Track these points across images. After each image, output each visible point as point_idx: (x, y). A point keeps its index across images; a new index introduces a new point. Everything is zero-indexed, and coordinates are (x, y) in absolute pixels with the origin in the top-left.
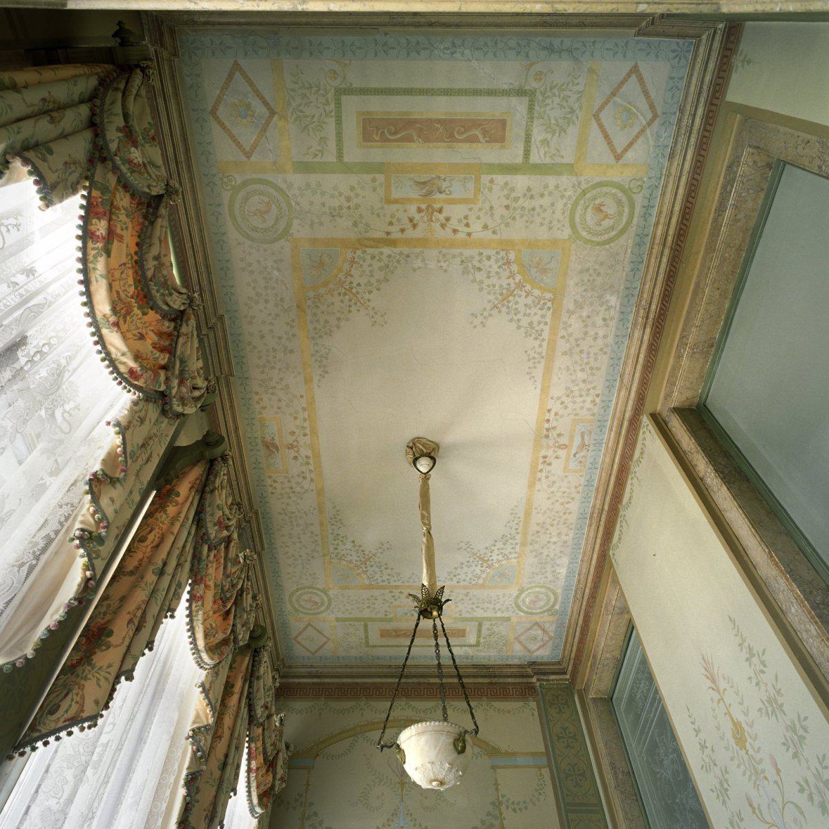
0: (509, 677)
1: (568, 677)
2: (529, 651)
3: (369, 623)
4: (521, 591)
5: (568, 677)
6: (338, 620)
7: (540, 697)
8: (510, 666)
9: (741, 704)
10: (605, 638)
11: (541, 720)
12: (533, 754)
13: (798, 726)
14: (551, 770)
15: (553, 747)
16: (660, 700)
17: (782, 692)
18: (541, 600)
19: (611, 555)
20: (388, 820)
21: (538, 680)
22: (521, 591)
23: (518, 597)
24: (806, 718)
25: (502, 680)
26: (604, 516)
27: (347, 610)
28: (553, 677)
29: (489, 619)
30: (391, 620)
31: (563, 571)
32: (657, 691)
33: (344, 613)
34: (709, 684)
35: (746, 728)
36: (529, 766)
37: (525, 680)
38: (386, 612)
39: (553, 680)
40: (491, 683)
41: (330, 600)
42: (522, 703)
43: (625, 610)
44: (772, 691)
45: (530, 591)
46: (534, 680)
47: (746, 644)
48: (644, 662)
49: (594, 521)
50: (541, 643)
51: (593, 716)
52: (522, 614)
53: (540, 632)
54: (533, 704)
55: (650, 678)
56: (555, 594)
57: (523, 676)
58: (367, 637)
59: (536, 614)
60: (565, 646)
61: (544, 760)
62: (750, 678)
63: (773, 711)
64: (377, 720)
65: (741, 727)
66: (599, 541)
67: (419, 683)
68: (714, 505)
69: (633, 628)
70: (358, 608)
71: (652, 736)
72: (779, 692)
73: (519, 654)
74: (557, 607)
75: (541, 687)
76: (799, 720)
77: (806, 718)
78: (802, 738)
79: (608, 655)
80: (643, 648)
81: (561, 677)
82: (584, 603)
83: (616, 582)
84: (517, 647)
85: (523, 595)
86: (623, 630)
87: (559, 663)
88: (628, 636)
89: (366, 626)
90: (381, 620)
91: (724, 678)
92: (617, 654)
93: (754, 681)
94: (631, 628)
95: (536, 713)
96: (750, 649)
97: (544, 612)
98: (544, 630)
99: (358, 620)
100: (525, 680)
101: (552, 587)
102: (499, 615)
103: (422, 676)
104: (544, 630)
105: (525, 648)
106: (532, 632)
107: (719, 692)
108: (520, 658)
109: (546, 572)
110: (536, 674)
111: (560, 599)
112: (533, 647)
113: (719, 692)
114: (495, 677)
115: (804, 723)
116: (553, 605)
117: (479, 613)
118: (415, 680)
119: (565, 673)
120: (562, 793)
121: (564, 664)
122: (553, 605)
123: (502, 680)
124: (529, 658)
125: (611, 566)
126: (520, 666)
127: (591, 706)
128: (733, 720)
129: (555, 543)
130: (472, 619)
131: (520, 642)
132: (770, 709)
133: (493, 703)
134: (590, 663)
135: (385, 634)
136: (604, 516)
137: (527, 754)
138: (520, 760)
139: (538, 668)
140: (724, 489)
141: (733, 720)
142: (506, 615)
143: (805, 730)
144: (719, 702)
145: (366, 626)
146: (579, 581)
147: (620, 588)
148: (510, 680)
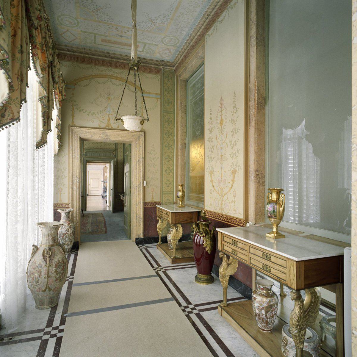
0: (152, 64)
1: (174, 68)
2: (162, 57)
3: (96, 35)
4: (165, 37)
5: (174, 68)
6: (82, 31)
7: (162, 74)
8: (153, 60)
9: (226, 116)
10: (192, 63)
11: (161, 82)
12: (156, 94)
13: (237, 130)
14: (161, 100)
15: (163, 93)
16: (204, 92)
17: (237, 120)
18: (172, 41)
19: (206, 38)
20: (104, 109)
21: (163, 68)
22: (165, 37)
23: (164, 38)
24: (239, 130)
25: (149, 65)
26: (209, 19)
27: (86, 28)
28: (168, 67)
29: (149, 44)
30: (106, 36)
31: (184, 33)
32: (203, 89)
33: (85, 29)
34: (220, 105)
35: (224, 122)
36: (154, 98)
37: (158, 67)
38: (105, 32)
39: (168, 69)
40: (145, 66)
41: (78, 23)
42: (155, 76)
43: (203, 58)
44: (235, 119)
45: (169, 37)
46: (161, 67)
47: (235, 103)
48: (203, 77)
49: (204, 18)
50: (168, 55)
51: (179, 86)
52: (163, 45)
53: (169, 52)
54: (159, 76)
55: (203, 84)
56: (178, 40)
57: (157, 65)
58: (95, 40)
59: (169, 45)
60: (176, 58)
61: (159, 97)
62: (231, 112)
63: (233, 123)
64: (98, 74)
65: (223, 121)
66: (203, 27)
67: (117, 62)
68: (249, 51)
69: (204, 64)
70: (92, 29)
71: (196, 101)
72: (237, 120)
73: (158, 57)
74: (178, 45)
75: (163, 70)
76: (238, 129)
77: (239, 130)
78: (236, 133)
79: (191, 69)
80: (204, 73)
81: (172, 68)
82: (189, 47)
83: (203, 48)
84: (158, 55)
85: (165, 39)
86: (199, 63)
87: (172, 62)
88: (200, 66)
89: (95, 36)
90: (103, 35)
91: (225, 107)
92: (194, 69)
93: (232, 113)
94: (203, 63)
95: (160, 80)
96: (235, 105)
97: (172, 45)
98: (170, 51)
99: (92, 33)
100: (158, 67)
101: (178, 38)
102: (154, 43)
103: (118, 59)
104: (170, 51)
105: (161, 56)
106: (165, 51)
107: (222, 109)
108: (158, 58)
109: (178, 32)
110: (163, 65)
111: (179, 43)
112: (164, 56)
113: (222, 109)
114: (147, 64)
115: (238, 130)
116: (177, 44)
117: (146, 41)
118: (115, 60)
119: (174, 67)
120: (163, 107)
121: (174, 64)
122: (177, 44)
123: (149, 65)
124: (161, 59)
125: (204, 40)
126: (157, 61)
127: (180, 82)
128: (222, 118)
129: (185, 22)
130: (142, 43)
131: (160, 54)
132: (232, 122)
133: (144, 74)
134: (183, 68)
135: (103, 41)
136: (209, 19)
137: (154, 93)
138: (152, 95)
139: (164, 63)
140: (255, 48)
141: (222, 118)
142: (156, 44)
143: (238, 132)
144: (220, 111)
145: (95, 36)
146: (189, 38)
147: (205, 51)
148: (152, 66)
